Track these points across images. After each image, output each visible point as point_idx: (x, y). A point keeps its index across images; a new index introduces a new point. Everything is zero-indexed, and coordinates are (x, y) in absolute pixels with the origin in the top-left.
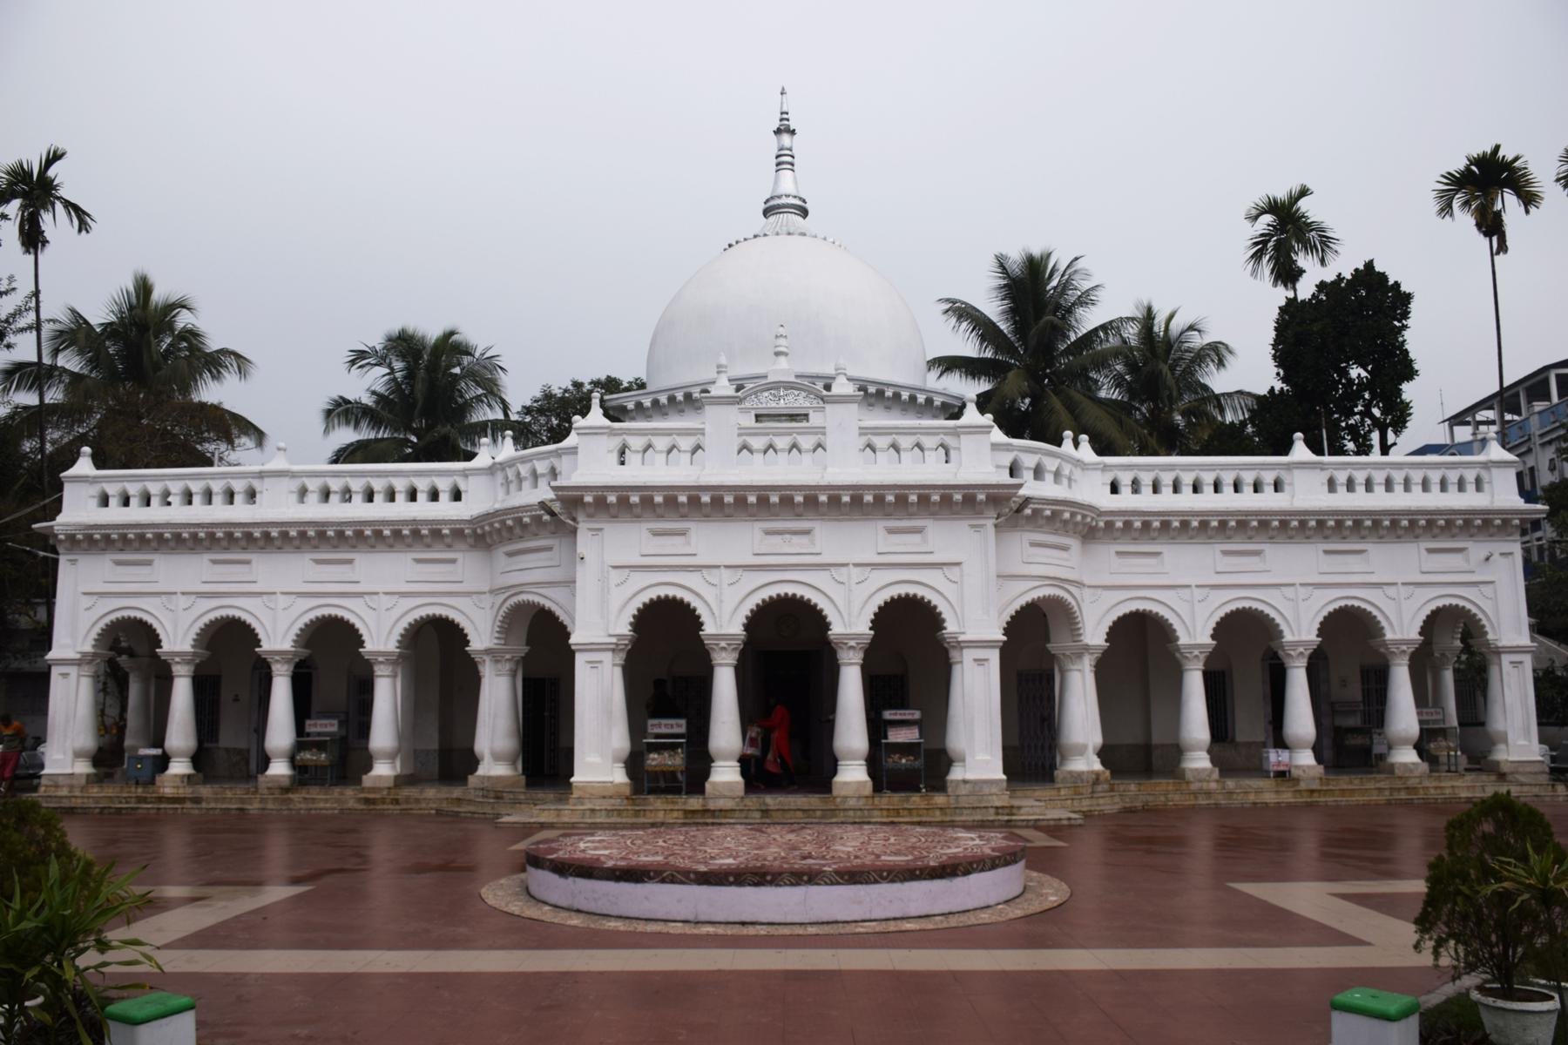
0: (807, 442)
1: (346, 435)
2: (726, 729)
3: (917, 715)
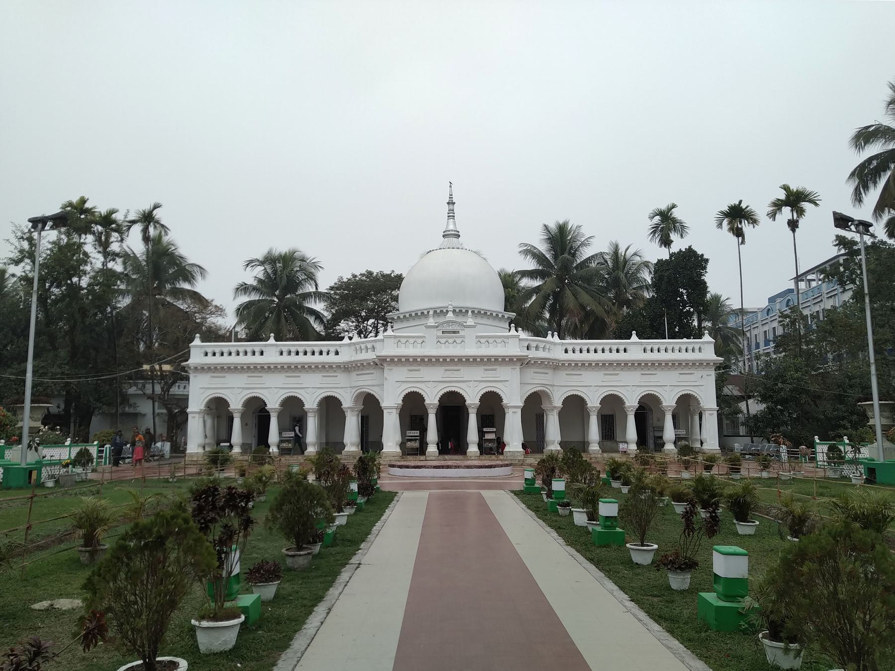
0: (459, 340)
1: (244, 299)
2: (432, 435)
3: (494, 430)
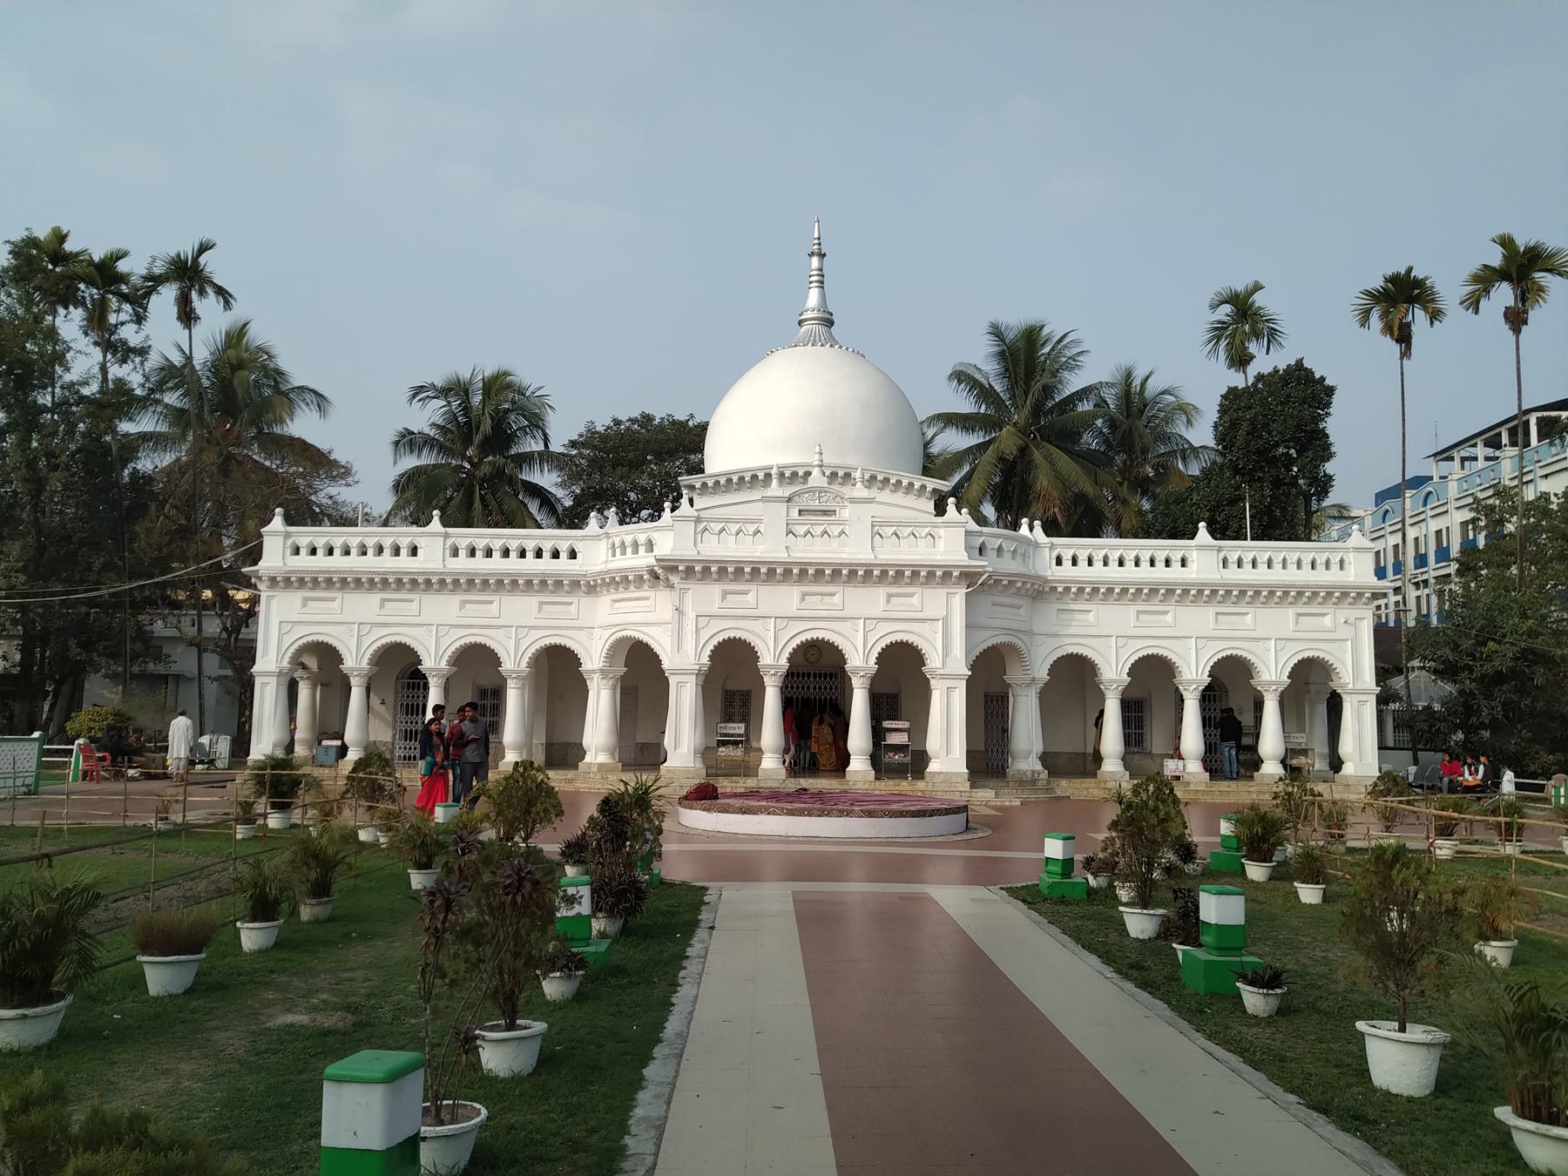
0: (835, 530)
3: (906, 725)
